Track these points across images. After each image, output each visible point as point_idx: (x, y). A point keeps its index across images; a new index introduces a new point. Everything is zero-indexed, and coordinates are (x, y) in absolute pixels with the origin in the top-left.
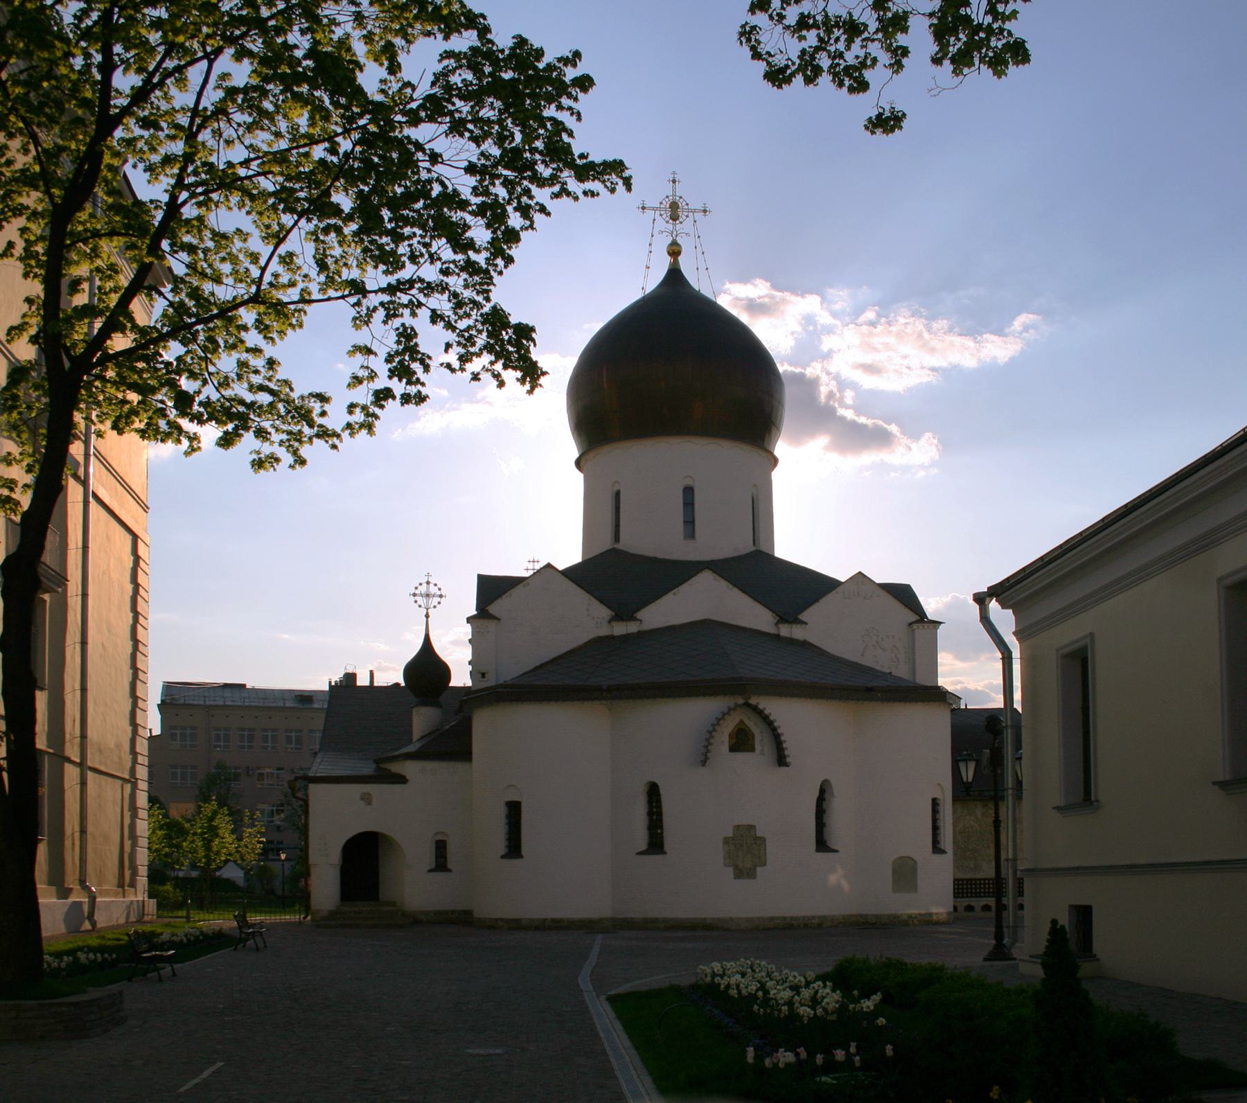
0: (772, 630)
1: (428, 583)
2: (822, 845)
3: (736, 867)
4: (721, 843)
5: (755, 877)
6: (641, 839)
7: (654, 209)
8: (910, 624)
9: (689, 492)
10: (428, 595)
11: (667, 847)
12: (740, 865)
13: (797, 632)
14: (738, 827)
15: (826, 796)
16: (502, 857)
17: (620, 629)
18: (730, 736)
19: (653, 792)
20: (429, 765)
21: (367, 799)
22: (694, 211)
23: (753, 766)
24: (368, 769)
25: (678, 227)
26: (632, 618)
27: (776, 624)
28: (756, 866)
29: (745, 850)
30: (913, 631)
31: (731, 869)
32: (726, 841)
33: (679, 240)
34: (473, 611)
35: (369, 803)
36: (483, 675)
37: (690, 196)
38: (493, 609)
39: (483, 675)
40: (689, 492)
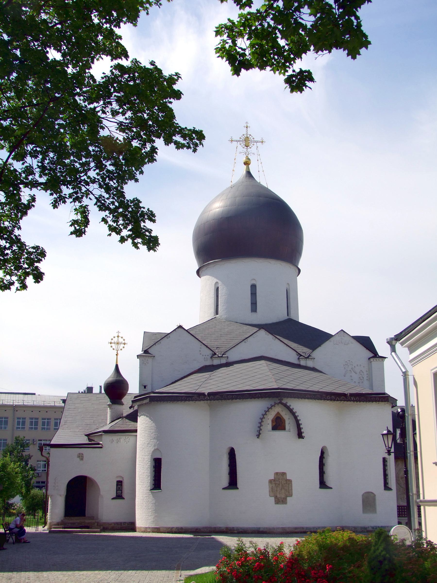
0: (296, 362)
2: (323, 484)
3: (276, 497)
6: (225, 480)
7: (237, 141)
8: (369, 359)
9: (253, 287)
10: (118, 343)
11: (239, 486)
12: (278, 496)
13: (310, 363)
14: (277, 474)
15: (325, 456)
18: (272, 421)
19: (232, 454)
22: (257, 142)
23: (285, 438)
25: (249, 150)
27: (299, 359)
28: (287, 496)
29: (281, 487)
30: (371, 362)
32: (271, 481)
33: (250, 157)
34: (140, 352)
36: (145, 387)
37: (255, 134)
39: (145, 387)
40: (253, 287)
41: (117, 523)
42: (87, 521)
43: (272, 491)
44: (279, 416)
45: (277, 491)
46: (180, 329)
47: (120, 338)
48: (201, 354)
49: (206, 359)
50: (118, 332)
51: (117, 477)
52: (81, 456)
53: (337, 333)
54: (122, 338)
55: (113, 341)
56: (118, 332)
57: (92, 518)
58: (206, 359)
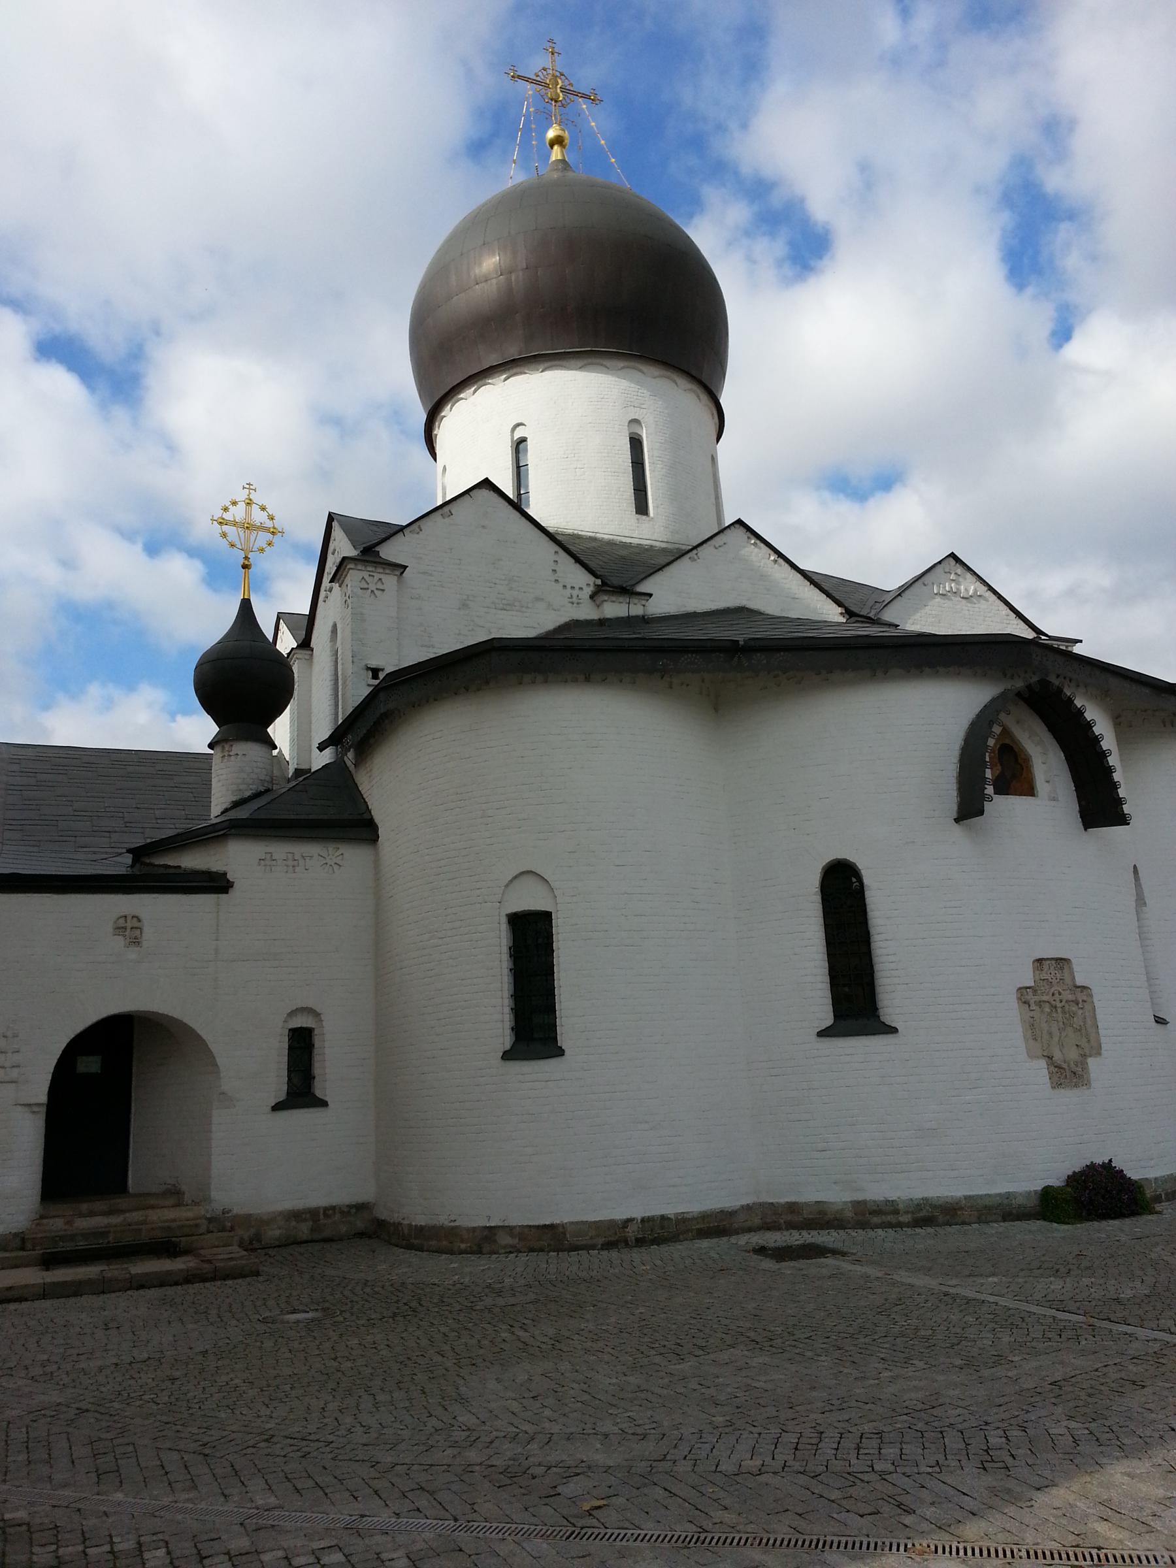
1: (249, 503)
4: (1013, 1003)
5: (1087, 1084)
6: (816, 1002)
12: (1058, 1056)
16: (507, 1056)
17: (614, 609)
20: (281, 850)
21: (130, 930)
24: (121, 865)
26: (626, 591)
28: (1084, 1056)
31: (1043, 1063)
35: (136, 942)
38: (388, 552)
41: (296, 1215)
42: (164, 1216)
43: (1035, 1039)
44: (1007, 741)
45: (1050, 1034)
46: (485, 493)
47: (255, 508)
48: (557, 581)
49: (575, 599)
50: (249, 486)
51: (293, 1013)
52: (130, 930)
53: (940, 562)
54: (263, 509)
55: (228, 516)
56: (249, 486)
57: (175, 1194)
58: (575, 599)
